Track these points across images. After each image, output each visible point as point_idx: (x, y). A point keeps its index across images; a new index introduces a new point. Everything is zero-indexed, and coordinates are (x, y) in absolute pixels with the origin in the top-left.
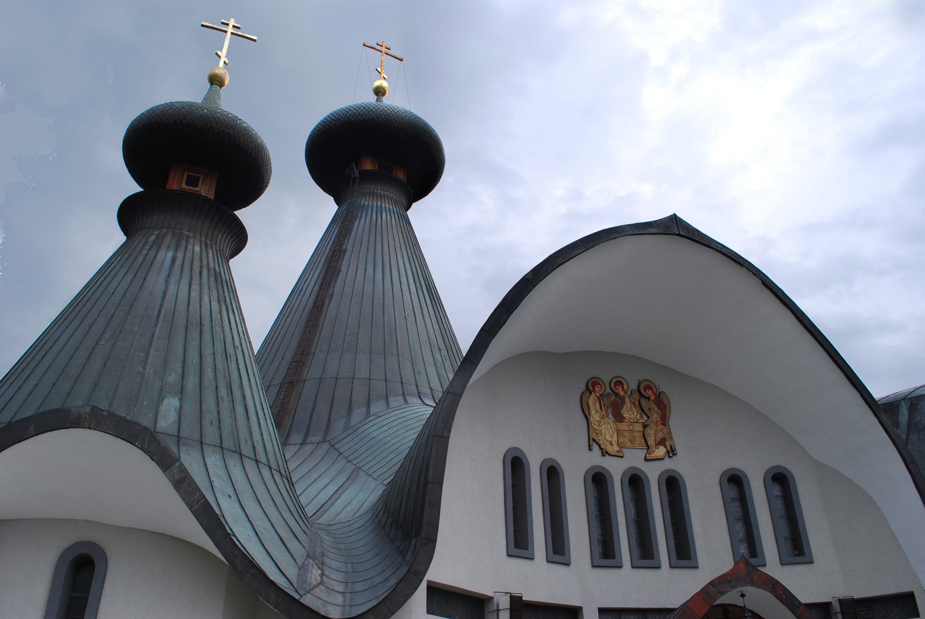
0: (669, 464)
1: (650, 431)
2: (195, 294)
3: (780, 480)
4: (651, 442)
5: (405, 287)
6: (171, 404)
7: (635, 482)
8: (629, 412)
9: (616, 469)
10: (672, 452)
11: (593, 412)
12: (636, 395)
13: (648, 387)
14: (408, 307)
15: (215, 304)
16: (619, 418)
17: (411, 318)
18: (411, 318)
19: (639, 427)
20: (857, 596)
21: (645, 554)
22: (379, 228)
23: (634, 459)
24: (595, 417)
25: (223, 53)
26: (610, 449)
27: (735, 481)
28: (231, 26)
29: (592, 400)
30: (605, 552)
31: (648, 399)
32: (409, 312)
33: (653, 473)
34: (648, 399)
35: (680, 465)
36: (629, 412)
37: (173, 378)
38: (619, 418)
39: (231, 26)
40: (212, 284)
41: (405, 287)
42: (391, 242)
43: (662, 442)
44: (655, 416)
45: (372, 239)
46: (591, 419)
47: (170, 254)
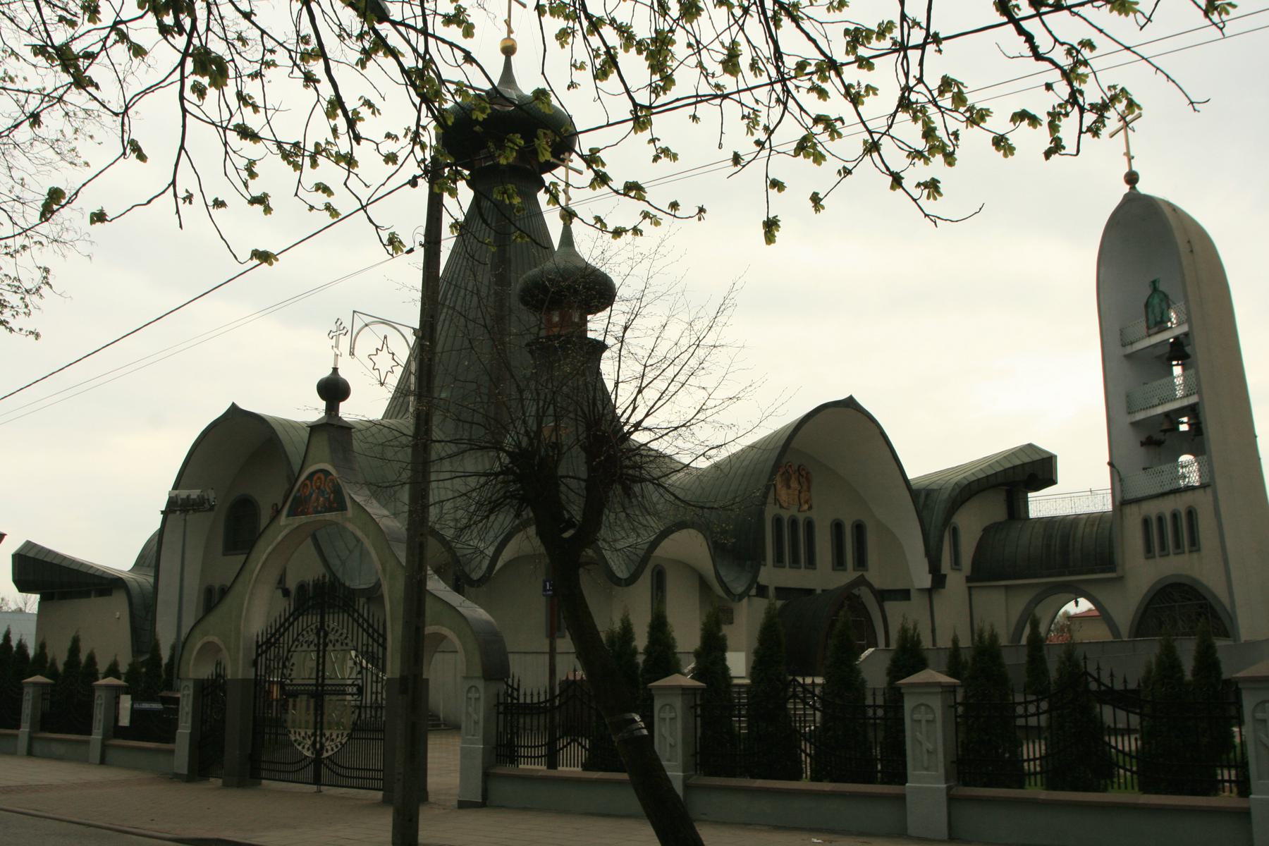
0: (808, 514)
3: (859, 529)
7: (794, 522)
8: (794, 484)
9: (786, 515)
10: (810, 508)
16: (789, 487)
20: (885, 587)
21: (795, 561)
23: (794, 511)
26: (785, 505)
27: (838, 527)
30: (779, 561)
33: (801, 518)
35: (813, 514)
36: (794, 484)
38: (789, 487)
43: (806, 502)
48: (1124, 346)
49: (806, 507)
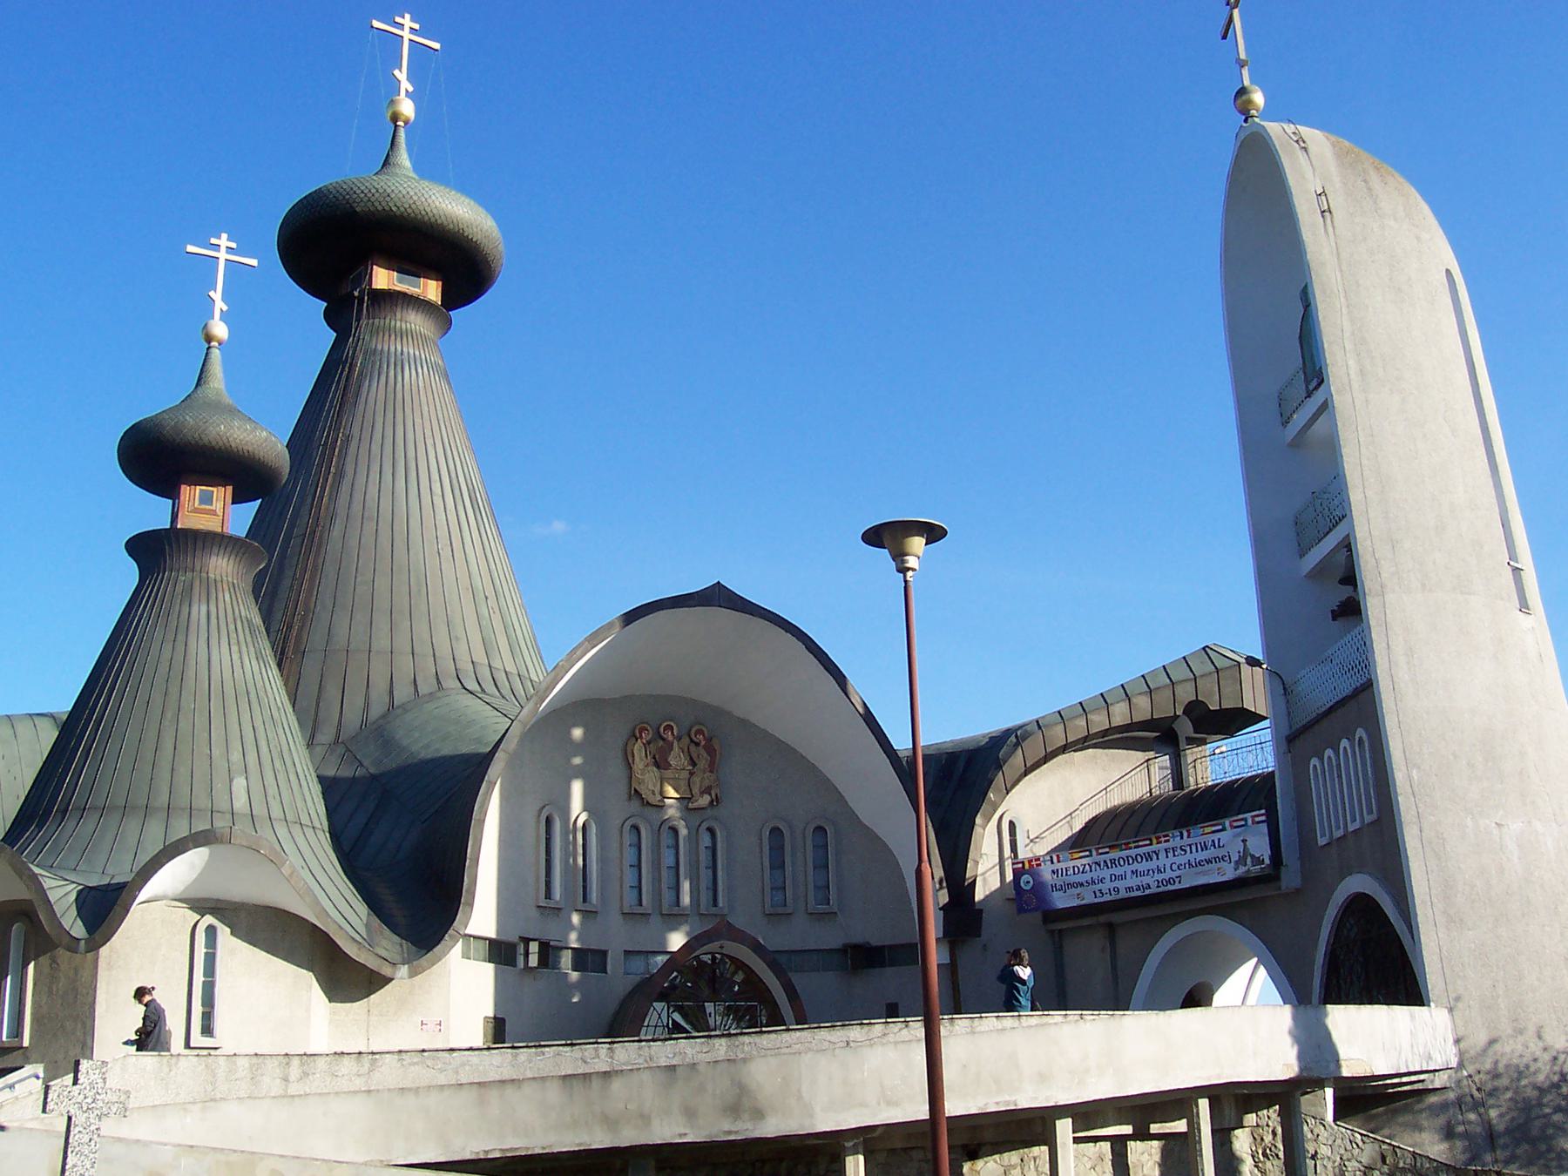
1: (696, 779)
2: (236, 656)
4: (696, 791)
5: (438, 500)
6: (240, 783)
8: (677, 759)
11: (637, 759)
12: (686, 740)
13: (699, 732)
14: (443, 532)
15: (254, 663)
17: (446, 553)
18: (446, 553)
19: (685, 774)
22: (399, 396)
24: (639, 763)
25: (217, 295)
28: (223, 249)
29: (638, 749)
31: (697, 744)
32: (443, 532)
34: (697, 744)
37: (236, 756)
39: (223, 249)
40: (249, 639)
41: (438, 500)
42: (418, 421)
43: (707, 791)
44: (703, 763)
45: (390, 415)
46: (635, 768)
47: (204, 609)
48: (1285, 423)
49: (704, 800)
